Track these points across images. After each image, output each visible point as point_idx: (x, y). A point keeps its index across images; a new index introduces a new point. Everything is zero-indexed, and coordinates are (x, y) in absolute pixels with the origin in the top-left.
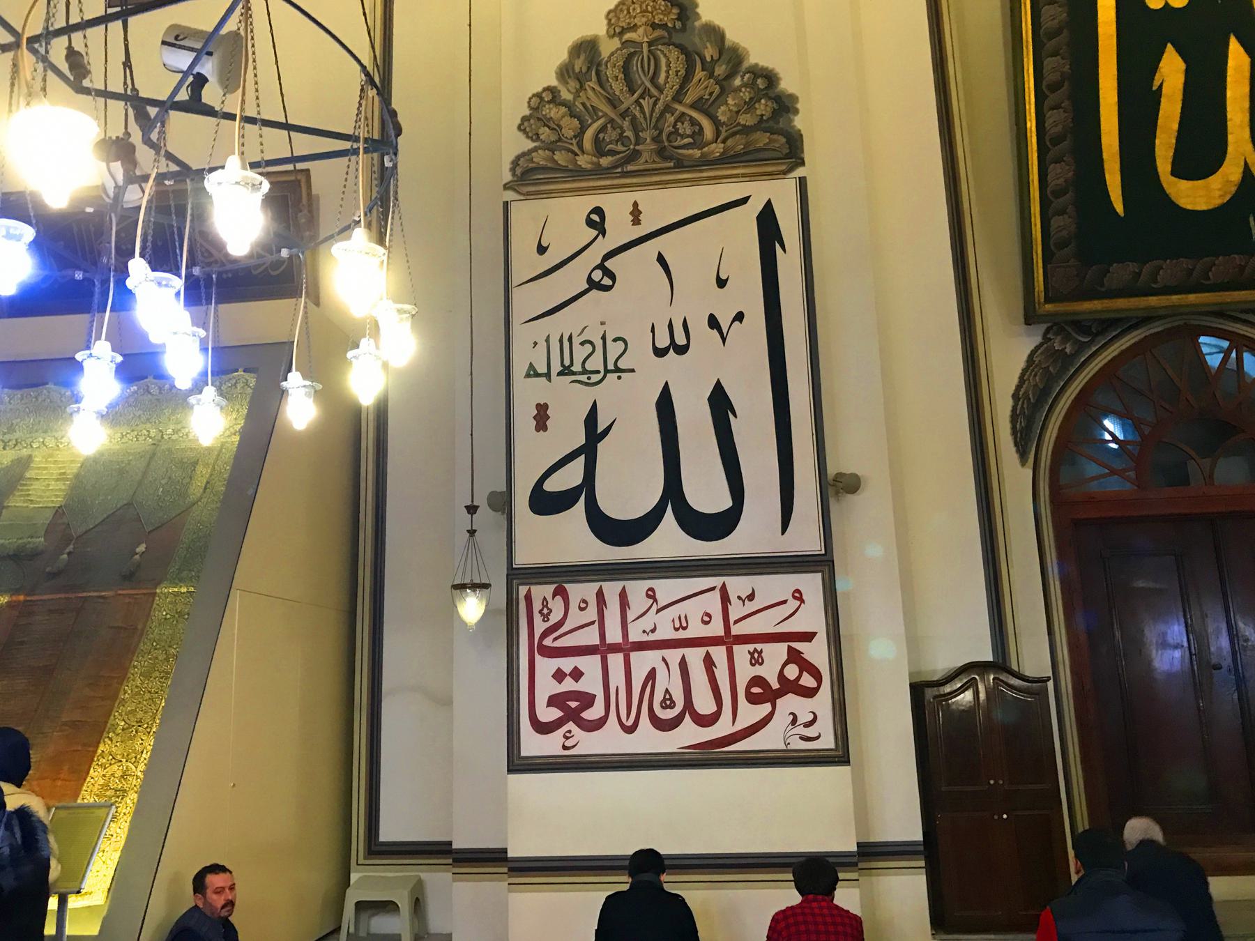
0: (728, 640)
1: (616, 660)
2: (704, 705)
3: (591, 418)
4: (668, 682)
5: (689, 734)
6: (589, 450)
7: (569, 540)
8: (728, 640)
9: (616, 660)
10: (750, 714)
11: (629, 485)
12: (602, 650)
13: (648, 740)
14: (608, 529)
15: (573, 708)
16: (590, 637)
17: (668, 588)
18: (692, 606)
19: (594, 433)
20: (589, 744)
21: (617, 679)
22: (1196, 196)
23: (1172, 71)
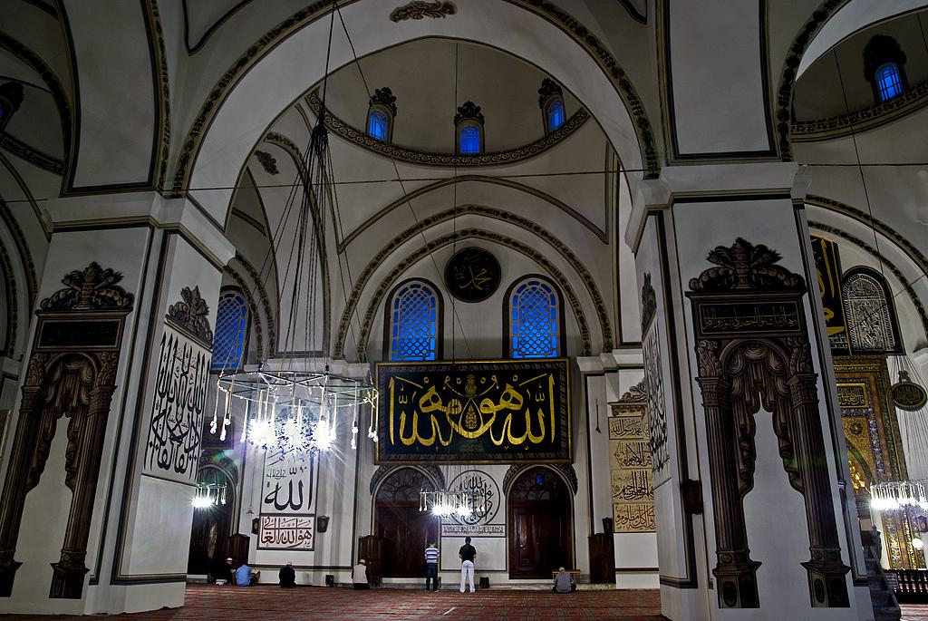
0: (297, 528)
1: (277, 531)
2: (291, 540)
3: (277, 486)
4: (286, 535)
5: (288, 545)
6: (276, 492)
7: (271, 508)
8: (297, 528)
9: (277, 531)
10: (299, 541)
11: (282, 501)
12: (275, 529)
13: (281, 545)
14: (277, 506)
15: (269, 539)
16: (273, 527)
17: (287, 518)
18: (291, 522)
19: (277, 489)
20: (271, 545)
21: (277, 534)
22: (407, 442)
23: (403, 416)
